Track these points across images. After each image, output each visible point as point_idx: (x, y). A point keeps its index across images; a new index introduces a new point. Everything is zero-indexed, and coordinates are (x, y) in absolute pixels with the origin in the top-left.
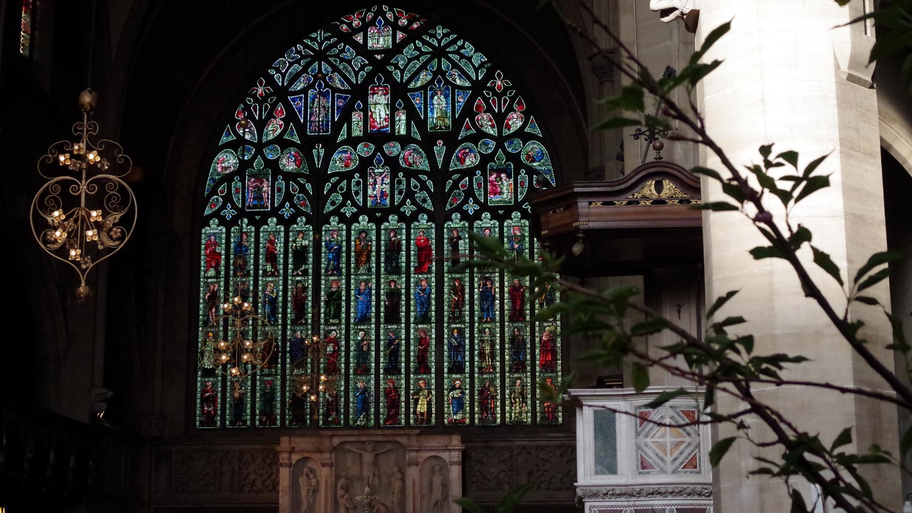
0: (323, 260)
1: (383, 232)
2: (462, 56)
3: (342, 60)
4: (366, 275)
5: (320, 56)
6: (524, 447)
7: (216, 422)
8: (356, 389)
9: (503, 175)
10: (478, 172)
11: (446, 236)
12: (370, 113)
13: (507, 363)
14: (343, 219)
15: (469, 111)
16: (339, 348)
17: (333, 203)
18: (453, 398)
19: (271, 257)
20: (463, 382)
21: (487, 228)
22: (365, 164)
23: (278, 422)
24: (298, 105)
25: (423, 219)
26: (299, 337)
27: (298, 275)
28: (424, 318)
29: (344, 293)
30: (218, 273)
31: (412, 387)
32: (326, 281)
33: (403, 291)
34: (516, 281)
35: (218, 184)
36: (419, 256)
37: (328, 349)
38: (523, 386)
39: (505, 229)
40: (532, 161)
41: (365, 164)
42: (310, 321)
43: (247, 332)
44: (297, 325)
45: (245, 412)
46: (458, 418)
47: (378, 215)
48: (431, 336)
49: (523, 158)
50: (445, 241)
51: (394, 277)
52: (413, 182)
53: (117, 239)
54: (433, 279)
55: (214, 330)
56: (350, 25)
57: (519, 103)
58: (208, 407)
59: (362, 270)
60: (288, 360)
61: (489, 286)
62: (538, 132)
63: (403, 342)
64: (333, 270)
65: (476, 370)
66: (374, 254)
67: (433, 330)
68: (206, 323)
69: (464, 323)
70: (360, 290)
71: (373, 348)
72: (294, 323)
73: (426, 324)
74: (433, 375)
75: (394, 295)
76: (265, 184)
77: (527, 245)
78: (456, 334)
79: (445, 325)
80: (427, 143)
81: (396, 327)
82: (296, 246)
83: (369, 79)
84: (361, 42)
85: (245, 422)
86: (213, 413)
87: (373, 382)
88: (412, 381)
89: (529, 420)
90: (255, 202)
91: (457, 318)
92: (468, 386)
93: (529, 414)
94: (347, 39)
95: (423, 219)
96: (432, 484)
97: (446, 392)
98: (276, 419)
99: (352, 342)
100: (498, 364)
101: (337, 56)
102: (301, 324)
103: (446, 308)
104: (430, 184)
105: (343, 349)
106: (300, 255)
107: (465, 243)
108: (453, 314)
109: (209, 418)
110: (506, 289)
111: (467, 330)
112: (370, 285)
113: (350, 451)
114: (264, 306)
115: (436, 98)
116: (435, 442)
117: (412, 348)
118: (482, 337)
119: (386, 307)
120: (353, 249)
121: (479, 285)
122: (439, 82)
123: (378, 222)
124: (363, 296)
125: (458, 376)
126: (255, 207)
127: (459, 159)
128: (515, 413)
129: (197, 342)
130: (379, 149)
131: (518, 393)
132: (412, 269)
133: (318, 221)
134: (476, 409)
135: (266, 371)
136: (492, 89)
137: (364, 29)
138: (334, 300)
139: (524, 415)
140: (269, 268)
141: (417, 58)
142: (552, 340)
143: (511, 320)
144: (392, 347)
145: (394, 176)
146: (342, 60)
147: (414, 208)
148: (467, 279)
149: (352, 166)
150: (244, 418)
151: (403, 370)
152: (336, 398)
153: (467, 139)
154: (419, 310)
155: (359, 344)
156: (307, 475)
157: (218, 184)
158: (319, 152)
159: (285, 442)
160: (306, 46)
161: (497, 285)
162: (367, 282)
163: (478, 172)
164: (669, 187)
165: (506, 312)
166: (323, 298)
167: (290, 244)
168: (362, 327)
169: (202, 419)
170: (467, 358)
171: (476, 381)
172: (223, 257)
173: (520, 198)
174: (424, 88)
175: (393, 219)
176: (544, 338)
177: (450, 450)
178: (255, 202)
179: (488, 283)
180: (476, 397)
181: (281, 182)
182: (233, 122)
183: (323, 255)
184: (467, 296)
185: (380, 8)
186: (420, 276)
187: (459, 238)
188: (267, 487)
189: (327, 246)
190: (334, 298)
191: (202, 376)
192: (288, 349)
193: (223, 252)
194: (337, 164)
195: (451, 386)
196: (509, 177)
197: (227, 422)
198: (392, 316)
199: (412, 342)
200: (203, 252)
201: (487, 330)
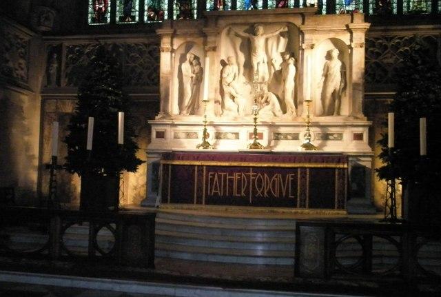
23: (166, 17)
45: (134, 8)
46: (351, 9)
58: (100, 4)
85: (134, 17)
86: (103, 9)
89: (430, 9)
96: (328, 71)
109: (100, 15)
150: (132, 14)
156: (191, 63)
169: (94, 16)
188: (153, 80)
197: (117, 19)
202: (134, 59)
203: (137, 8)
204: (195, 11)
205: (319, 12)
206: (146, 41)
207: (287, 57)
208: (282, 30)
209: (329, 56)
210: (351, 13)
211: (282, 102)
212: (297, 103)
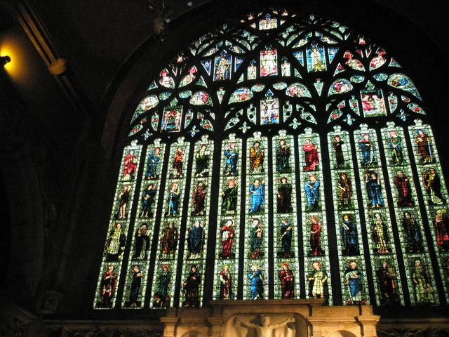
0: (222, 165)
1: (274, 142)
4: (260, 174)
7: (112, 303)
8: (251, 272)
9: (375, 97)
11: (329, 142)
12: (261, 66)
13: (402, 244)
15: (339, 58)
16: (234, 235)
18: (350, 279)
19: (178, 165)
20: (359, 263)
21: (366, 134)
23: (172, 304)
24: (207, 65)
26: (197, 226)
27: (199, 177)
28: (315, 207)
29: (239, 189)
30: (132, 177)
31: (306, 269)
32: (224, 180)
33: (294, 186)
34: (399, 173)
37: (224, 236)
38: (424, 266)
39: (383, 134)
40: (397, 86)
41: (257, 99)
42: (208, 213)
43: (151, 223)
44: (196, 216)
45: (141, 294)
48: (322, 222)
49: (389, 83)
50: (330, 146)
51: (285, 175)
52: (298, 107)
54: (321, 175)
55: (122, 221)
58: (107, 289)
59: (256, 170)
60: (186, 247)
61: (374, 178)
63: (296, 229)
64: (230, 172)
65: (371, 252)
66: (266, 158)
67: (325, 218)
68: (117, 217)
69: (354, 210)
70: (254, 186)
71: (267, 235)
72: (193, 215)
73: (317, 212)
74: (327, 258)
75: (285, 190)
76: (178, 114)
77: (405, 145)
78: (347, 220)
79: (336, 212)
81: (288, 215)
82: (199, 156)
85: (139, 304)
87: (267, 265)
88: (306, 264)
89: (438, 301)
90: (169, 127)
91: (347, 206)
92: (364, 268)
93: (436, 295)
95: (309, 131)
97: (342, 274)
99: (246, 230)
100: (393, 245)
102: (200, 215)
103: (335, 198)
104: (313, 107)
105: (238, 236)
106: (202, 163)
107: (348, 146)
108: (343, 202)
109: (106, 299)
110: (391, 180)
111: (358, 216)
112: (263, 182)
113: (243, 325)
114: (168, 201)
115: (312, 53)
117: (304, 233)
118: (373, 221)
119: (278, 199)
120: (248, 155)
121: (365, 178)
124: (257, 191)
125: (353, 258)
126: (168, 130)
127: (335, 89)
128: (420, 294)
129: (107, 231)
131: (421, 273)
132: (301, 168)
134: (376, 290)
137: (257, 21)
138: (231, 195)
139: (430, 296)
140: (175, 172)
143: (401, 205)
144: (285, 233)
145: (282, 104)
146: (241, 38)
148: (353, 174)
149: (248, 98)
150: (138, 300)
151: (297, 254)
152: (230, 281)
153: (339, 76)
154: (309, 200)
155: (254, 235)
157: (141, 117)
158: (221, 93)
161: (382, 177)
162: (260, 180)
165: (394, 199)
166: (220, 194)
167: (195, 155)
168: (256, 217)
169: (100, 300)
170: (360, 241)
171: (372, 262)
172: (138, 166)
173: (392, 111)
174: (303, 49)
176: (437, 221)
178: (169, 127)
179: (372, 176)
180: (375, 278)
181: (191, 114)
183: (222, 161)
184: (354, 188)
186: (309, 173)
187: (341, 143)
189: (225, 155)
190: (230, 194)
191: (107, 261)
192: (187, 237)
193: (139, 162)
194: (236, 97)
195: (347, 267)
196: (380, 97)
197: (123, 304)
198: (284, 206)
199: (304, 228)
200: (122, 163)
201: (377, 215)
203: (144, 293)
204: (202, 298)
205: (326, 303)
208: (289, 321)
210: (359, 305)
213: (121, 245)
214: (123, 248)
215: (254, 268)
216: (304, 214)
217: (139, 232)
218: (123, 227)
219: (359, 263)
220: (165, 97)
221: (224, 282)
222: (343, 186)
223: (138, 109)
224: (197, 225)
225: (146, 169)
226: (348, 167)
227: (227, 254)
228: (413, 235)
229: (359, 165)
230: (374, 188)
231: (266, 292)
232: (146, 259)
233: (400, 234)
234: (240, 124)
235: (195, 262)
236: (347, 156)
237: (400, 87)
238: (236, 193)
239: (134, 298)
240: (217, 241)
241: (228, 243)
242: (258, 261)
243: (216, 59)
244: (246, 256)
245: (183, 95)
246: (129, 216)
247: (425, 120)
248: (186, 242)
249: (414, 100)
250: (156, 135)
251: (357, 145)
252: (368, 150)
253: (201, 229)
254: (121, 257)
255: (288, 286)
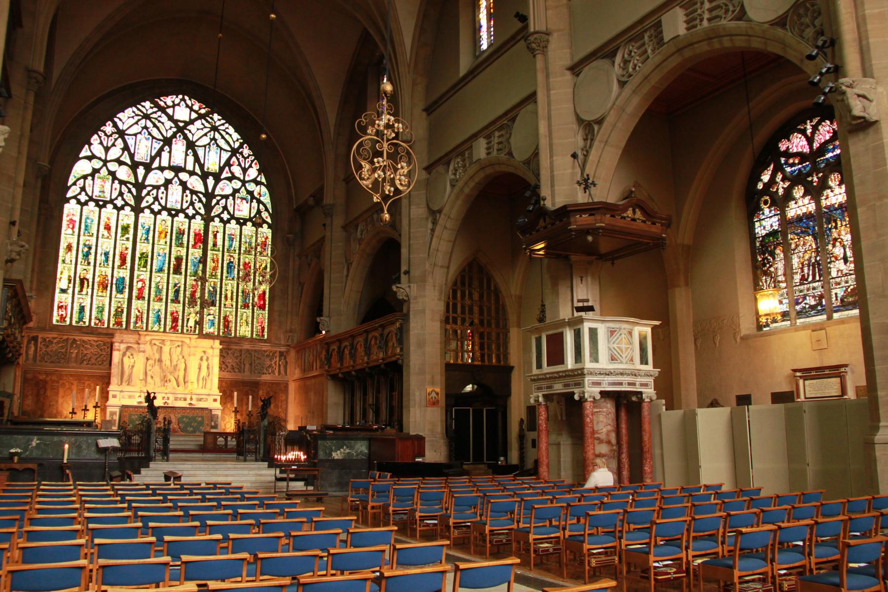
2: (227, 133)
3: (159, 121)
5: (147, 117)
6: (248, 350)
8: (154, 310)
10: (231, 198)
14: (152, 211)
15: (228, 164)
17: (147, 202)
19: (108, 228)
20: (215, 311)
22: (168, 182)
23: (106, 325)
24: (130, 141)
25: (198, 217)
30: (74, 232)
33: (184, 257)
35: (78, 179)
36: (195, 240)
41: (168, 182)
47: (173, 213)
53: (405, 186)
56: (165, 103)
57: (256, 164)
59: (162, 241)
62: (264, 180)
68: (64, 261)
71: (165, 287)
72: (119, 267)
78: (212, 285)
80: (204, 176)
83: (174, 135)
84: (171, 114)
85: (85, 322)
86: (64, 315)
87: (164, 307)
89: (250, 336)
94: (163, 110)
95: (198, 217)
97: (205, 316)
98: (104, 323)
100: (234, 304)
101: (156, 119)
105: (147, 285)
106: (125, 229)
109: (63, 318)
111: (219, 283)
113: (155, 344)
116: (207, 343)
120: (157, 230)
122: (213, 144)
123: (173, 216)
126: (100, 196)
130: (176, 175)
133: (137, 210)
135: (100, 294)
136: (241, 153)
137: (174, 106)
140: (106, 233)
141: (202, 129)
142: (264, 293)
145: (184, 192)
146: (159, 121)
147: (194, 212)
153: (226, 179)
157: (78, 179)
158: (141, 171)
159: (117, 338)
160: (139, 109)
163: (231, 198)
164: (639, 214)
171: (222, 312)
175: (181, 215)
177: (212, 348)
178: (100, 194)
181: (116, 185)
182: (90, 144)
185: (183, 97)
187: (217, 232)
192: (114, 282)
196: (247, 202)
197: (74, 323)
198: (177, 271)
202: (87, 349)
206: (95, 339)
207: (181, 357)
209: (201, 359)
211: (177, 380)
212: (185, 383)
213: (70, 283)
214: (71, 285)
215: (157, 308)
216: (188, 277)
217: (82, 275)
218: (69, 270)
219: (215, 311)
220: (97, 164)
221: (138, 314)
222: (214, 262)
223: (73, 171)
224: (121, 275)
225: (82, 226)
226: (219, 251)
227: (140, 297)
228: (246, 299)
229: (226, 250)
230: (231, 266)
231: (162, 322)
232: (87, 294)
233: (240, 297)
234: (153, 203)
235: (120, 300)
236: (219, 242)
237: (262, 199)
238: (147, 257)
239: (81, 319)
240: (134, 288)
241: (141, 290)
242: (159, 303)
243: (139, 136)
244: (151, 299)
245: (113, 166)
246: (74, 262)
247: (270, 227)
248: (114, 286)
249: (267, 210)
250: (91, 199)
251: (226, 235)
252: (233, 241)
253: (124, 278)
254: (70, 291)
255: (175, 320)
